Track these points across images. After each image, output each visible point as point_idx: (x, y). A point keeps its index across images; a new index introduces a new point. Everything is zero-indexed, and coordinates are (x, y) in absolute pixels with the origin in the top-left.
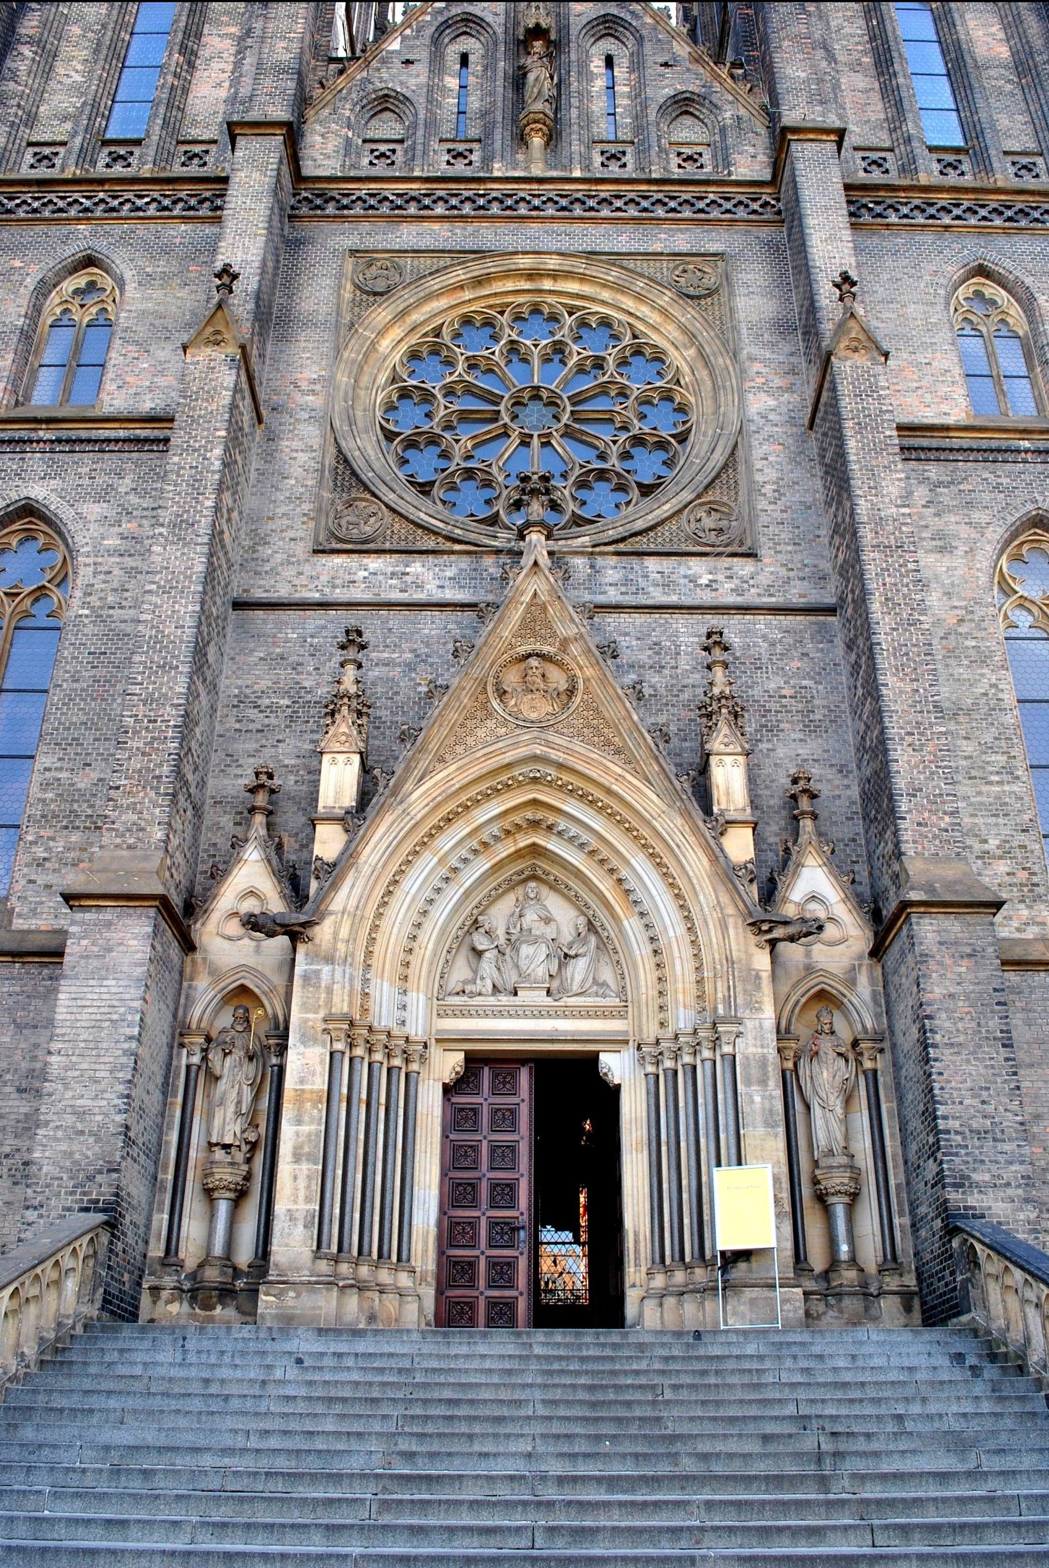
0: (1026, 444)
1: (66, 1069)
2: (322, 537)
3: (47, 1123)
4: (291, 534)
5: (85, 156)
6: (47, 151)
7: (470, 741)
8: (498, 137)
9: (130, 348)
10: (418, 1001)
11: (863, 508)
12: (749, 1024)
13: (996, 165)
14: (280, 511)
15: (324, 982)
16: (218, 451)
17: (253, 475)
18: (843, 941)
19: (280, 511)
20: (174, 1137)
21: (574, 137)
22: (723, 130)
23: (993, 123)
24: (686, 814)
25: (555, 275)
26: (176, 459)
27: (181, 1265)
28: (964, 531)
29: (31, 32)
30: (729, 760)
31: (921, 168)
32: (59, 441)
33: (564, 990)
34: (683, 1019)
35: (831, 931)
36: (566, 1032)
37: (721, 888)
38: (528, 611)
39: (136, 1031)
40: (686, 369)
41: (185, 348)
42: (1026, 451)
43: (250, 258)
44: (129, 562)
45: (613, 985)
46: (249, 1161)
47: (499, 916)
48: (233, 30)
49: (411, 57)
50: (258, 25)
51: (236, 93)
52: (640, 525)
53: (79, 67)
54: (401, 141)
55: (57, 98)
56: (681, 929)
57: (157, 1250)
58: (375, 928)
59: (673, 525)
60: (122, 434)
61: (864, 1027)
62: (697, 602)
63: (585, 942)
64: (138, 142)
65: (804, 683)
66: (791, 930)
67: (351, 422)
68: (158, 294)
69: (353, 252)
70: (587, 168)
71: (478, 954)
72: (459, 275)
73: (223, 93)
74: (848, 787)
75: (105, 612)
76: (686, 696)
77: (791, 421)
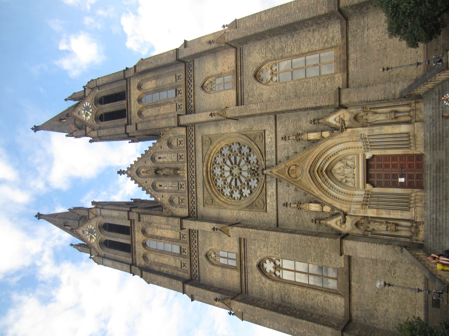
0: (239, 78)
1: (374, 255)
3: (385, 259)
5: (184, 257)
6: (183, 264)
7: (306, 183)
9: (225, 247)
10: (356, 192)
11: (258, 112)
12: (362, 132)
13: (179, 84)
14: (258, 218)
16: (250, 230)
18: (344, 114)
19: (258, 218)
20: (385, 237)
22: (175, 136)
23: (170, 84)
24: (320, 144)
25: (207, 168)
26: (252, 238)
27: (411, 236)
28: (258, 91)
29: (158, 268)
30: (308, 136)
32: (245, 260)
35: (342, 116)
36: (362, 165)
37: (335, 138)
38: (279, 173)
39: (367, 243)
40: (225, 143)
41: (229, 236)
42: (241, 78)
43: (209, 225)
44: (269, 246)
45: (352, 156)
46: (390, 223)
47: (339, 177)
48: (156, 230)
49: (161, 196)
50: (155, 225)
51: (170, 229)
52: (259, 152)
53: (164, 259)
55: (171, 263)
56: (342, 145)
57: (408, 240)
58: (343, 200)
59: (259, 146)
60: (243, 248)
61: (361, 110)
63: (344, 162)
64: (181, 247)
66: (343, 125)
67: (239, 205)
68: (214, 243)
69: (204, 206)
70: (184, 162)
71: (346, 181)
72: (208, 186)
73: (170, 231)
74: (312, 113)
75: (279, 251)
76: (294, 143)
77: (236, 124)
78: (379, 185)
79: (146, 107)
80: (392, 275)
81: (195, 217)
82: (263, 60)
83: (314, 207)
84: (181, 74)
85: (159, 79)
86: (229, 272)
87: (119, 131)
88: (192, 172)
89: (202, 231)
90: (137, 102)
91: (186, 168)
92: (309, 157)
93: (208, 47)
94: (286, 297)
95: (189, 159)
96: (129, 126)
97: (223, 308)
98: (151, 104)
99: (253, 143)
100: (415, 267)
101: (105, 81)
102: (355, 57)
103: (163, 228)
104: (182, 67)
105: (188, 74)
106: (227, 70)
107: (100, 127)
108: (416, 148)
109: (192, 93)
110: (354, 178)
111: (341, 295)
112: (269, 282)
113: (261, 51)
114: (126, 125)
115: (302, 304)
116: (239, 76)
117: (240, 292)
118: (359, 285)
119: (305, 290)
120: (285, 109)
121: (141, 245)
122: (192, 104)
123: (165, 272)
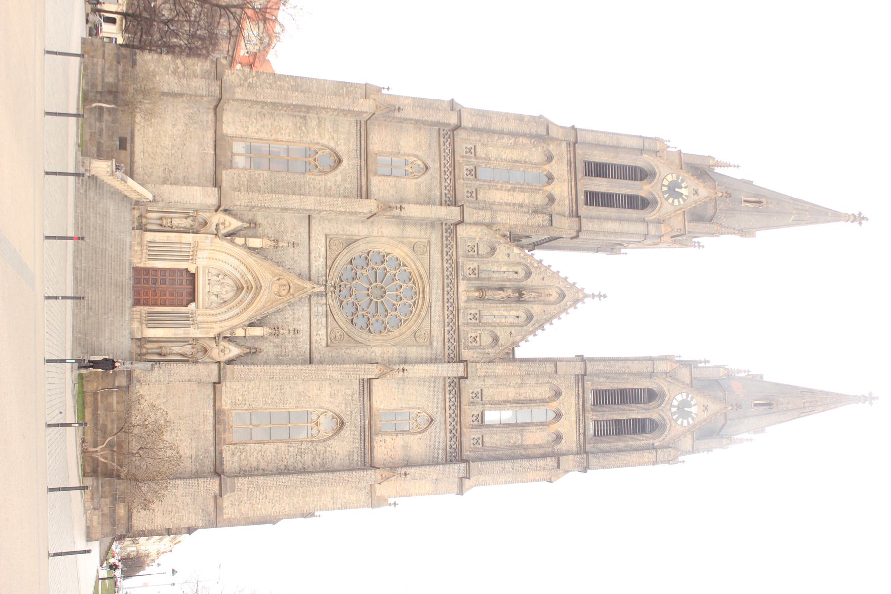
2: (331, 236)
4: (332, 229)
6: (473, 151)
8: (477, 282)
14: (339, 226)
15: (206, 241)
16: (342, 210)
17: (351, 218)
18: (219, 356)
21: (478, 304)
25: (423, 298)
26: (340, 200)
31: (470, 407)
32: (361, 167)
33: (210, 295)
34: (200, 319)
35: (222, 354)
44: (323, 189)
49: (511, 256)
50: (525, 210)
51: (495, 204)
52: (336, 317)
53: (509, 157)
54: (478, 254)
56: (221, 319)
57: (149, 209)
58: (220, 251)
59: (336, 325)
60: (363, 183)
62: (312, 330)
64: (476, 177)
65: (290, 356)
71: (218, 276)
72: (422, 271)
73: (498, 200)
76: (285, 326)
78: (179, 270)
79: (543, 401)
80: (167, 167)
81: (446, 224)
82: (329, 442)
83: (255, 243)
84: (473, 446)
85: (518, 445)
86: (388, 148)
87: (602, 366)
88: (450, 293)
89: (433, 204)
90: (563, 412)
91: (463, 297)
92: (262, 305)
93: (411, 471)
94: (299, 124)
95: (455, 313)
96: (577, 372)
97: (399, 96)
98: (533, 405)
99: (345, 330)
100: (143, 180)
101: (635, 456)
102: (206, 426)
103: (510, 206)
104: (466, 454)
105: (457, 443)
106: (387, 437)
107: (651, 377)
108: (140, 312)
109: (448, 412)
110: (209, 279)
111: (227, 136)
112: (324, 142)
113: (332, 457)
114: (584, 375)
115: (277, 118)
116: (366, 427)
117: (368, 122)
118: (205, 151)
119: (273, 137)
120: (291, 367)
121: (555, 176)
122: (448, 396)
123: (506, 136)
